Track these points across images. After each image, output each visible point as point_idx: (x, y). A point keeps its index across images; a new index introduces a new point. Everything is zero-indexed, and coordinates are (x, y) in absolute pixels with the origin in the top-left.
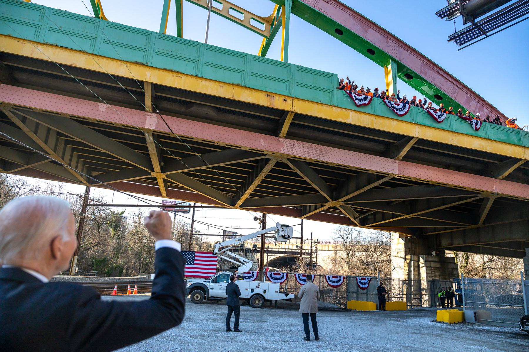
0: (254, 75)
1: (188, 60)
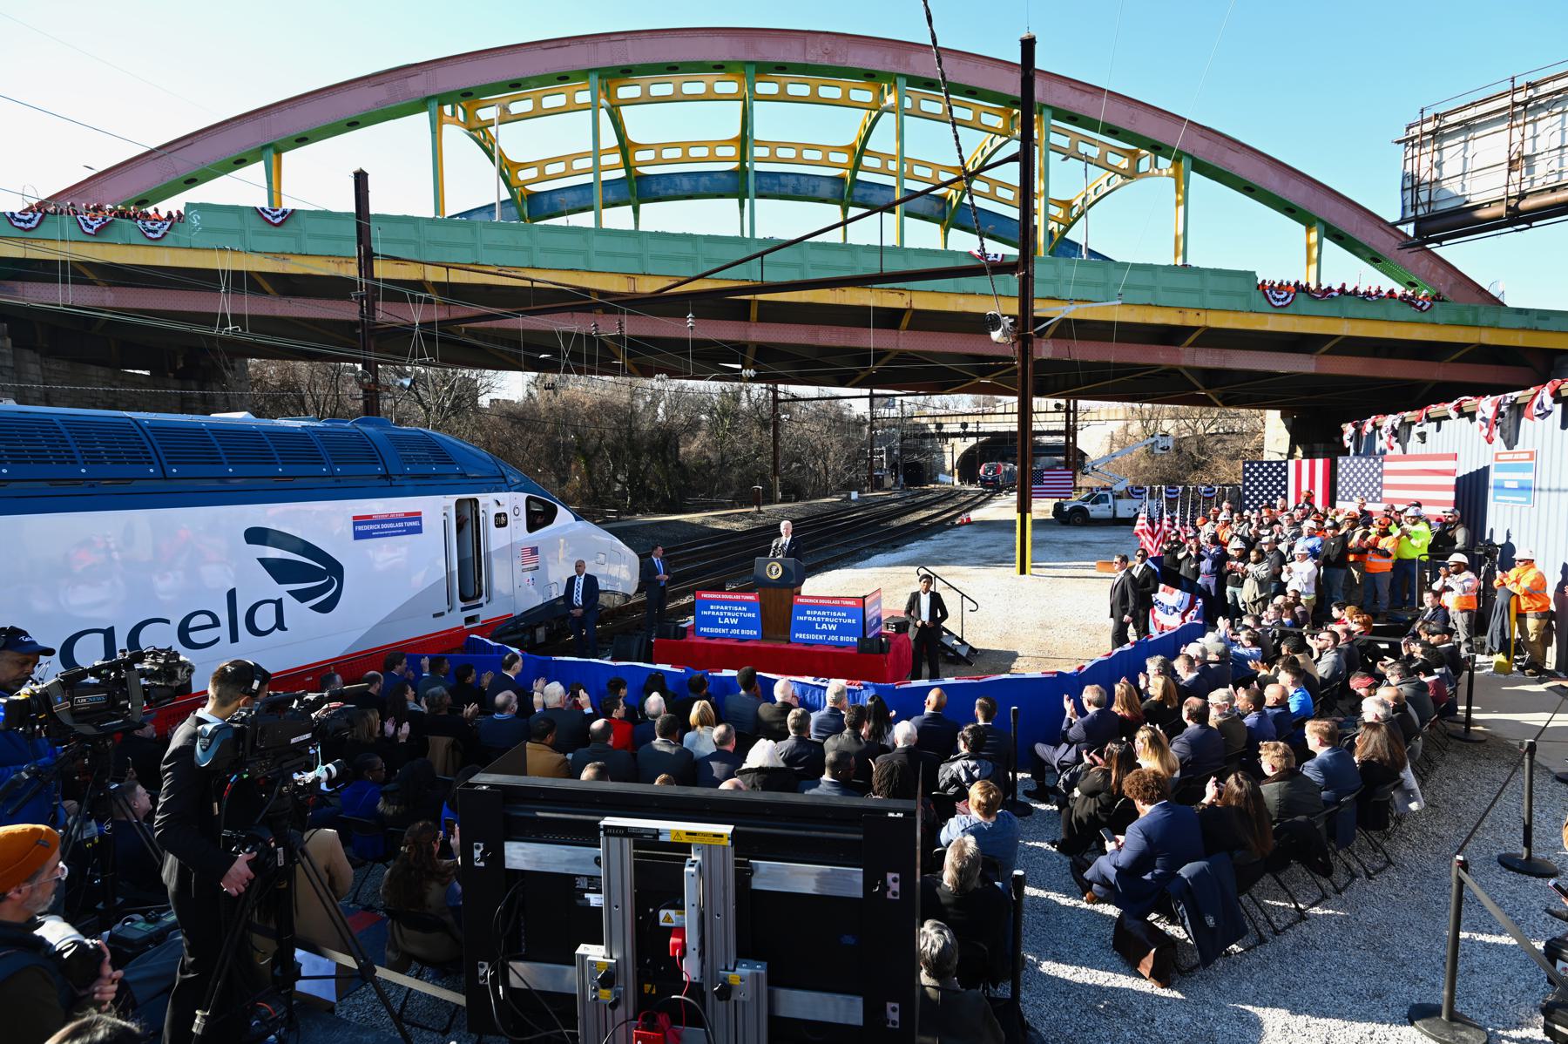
0: (1165, 289)
1: (1097, 285)
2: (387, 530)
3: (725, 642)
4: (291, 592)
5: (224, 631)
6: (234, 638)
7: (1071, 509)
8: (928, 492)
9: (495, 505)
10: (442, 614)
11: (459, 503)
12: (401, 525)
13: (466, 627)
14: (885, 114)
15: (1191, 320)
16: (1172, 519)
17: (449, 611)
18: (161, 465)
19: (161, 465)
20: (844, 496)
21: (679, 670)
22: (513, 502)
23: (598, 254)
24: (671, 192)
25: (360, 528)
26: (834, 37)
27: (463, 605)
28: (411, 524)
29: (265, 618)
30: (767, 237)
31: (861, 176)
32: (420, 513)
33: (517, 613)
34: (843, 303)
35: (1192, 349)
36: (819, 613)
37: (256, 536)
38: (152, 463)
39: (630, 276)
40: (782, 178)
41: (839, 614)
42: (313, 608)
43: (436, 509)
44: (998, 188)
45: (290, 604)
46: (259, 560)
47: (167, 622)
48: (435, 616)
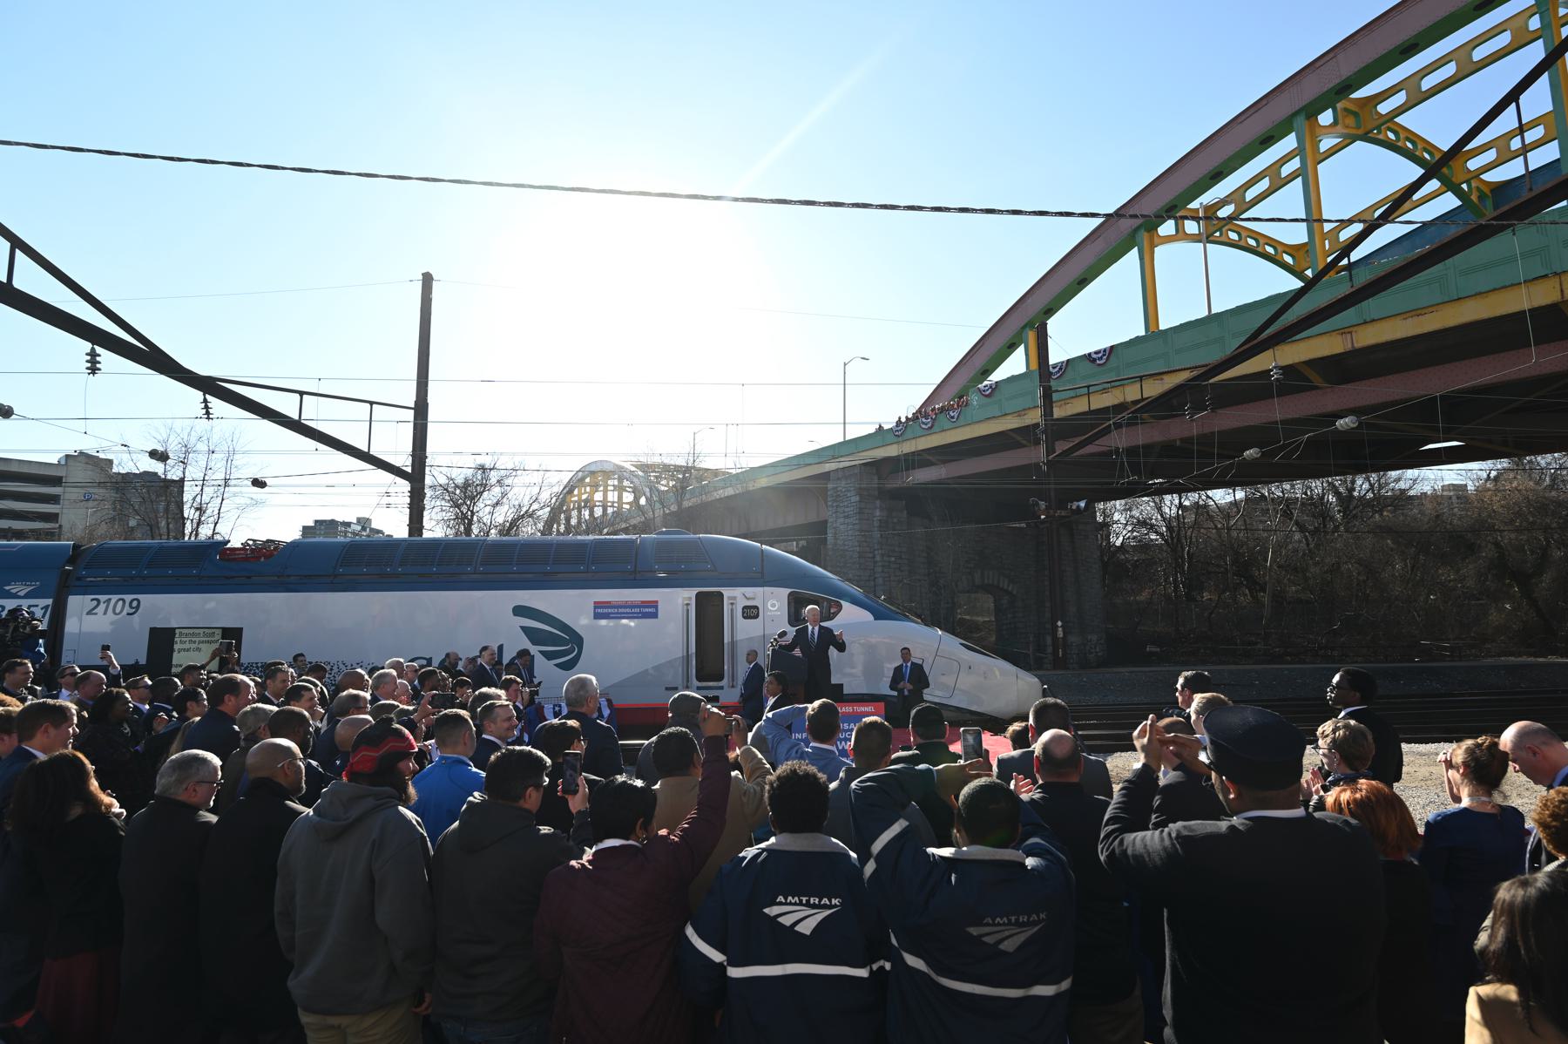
2: (624, 613)
11: (698, 595)
12: (638, 610)
28: (647, 610)
32: (657, 602)
37: (520, 611)
42: (556, 665)
46: (522, 627)
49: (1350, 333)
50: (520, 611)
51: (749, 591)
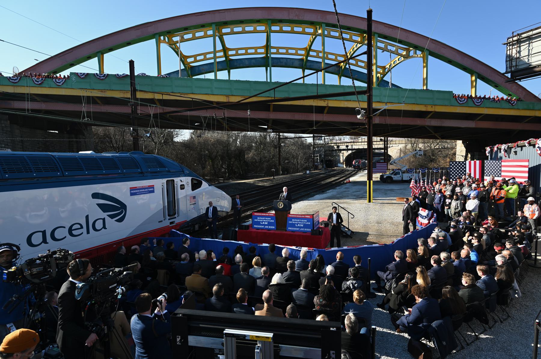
3: (263, 231)
4: (108, 215)
5: (84, 230)
6: (88, 232)
7: (386, 177)
8: (334, 170)
9: (180, 181)
10: (162, 221)
11: (167, 181)
12: (147, 190)
13: (170, 226)
14: (318, 36)
15: (430, 109)
16: (424, 182)
17: (164, 220)
18: (62, 172)
19: (62, 172)
20: (304, 172)
21: (247, 244)
22: (187, 180)
23: (216, 88)
24: (241, 65)
25: (132, 192)
26: (300, 10)
27: (169, 218)
28: (150, 189)
29: (99, 225)
30: (276, 81)
31: (309, 58)
32: (154, 186)
33: (188, 220)
34: (303, 104)
35: (430, 119)
36: (297, 220)
37: (95, 196)
38: (59, 171)
39: (227, 96)
40: (281, 59)
41: (304, 221)
42: (116, 221)
43: (159, 184)
44: (359, 62)
45: (108, 219)
46: (97, 204)
47: (64, 227)
48: (159, 222)
49: (228, 97)
50: (95, 196)
51: (182, 178)
